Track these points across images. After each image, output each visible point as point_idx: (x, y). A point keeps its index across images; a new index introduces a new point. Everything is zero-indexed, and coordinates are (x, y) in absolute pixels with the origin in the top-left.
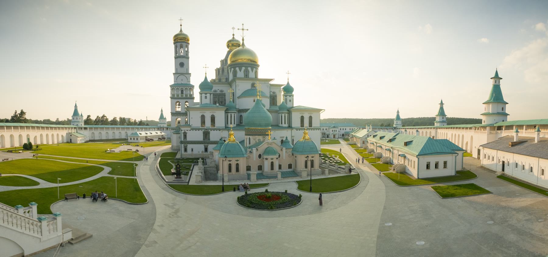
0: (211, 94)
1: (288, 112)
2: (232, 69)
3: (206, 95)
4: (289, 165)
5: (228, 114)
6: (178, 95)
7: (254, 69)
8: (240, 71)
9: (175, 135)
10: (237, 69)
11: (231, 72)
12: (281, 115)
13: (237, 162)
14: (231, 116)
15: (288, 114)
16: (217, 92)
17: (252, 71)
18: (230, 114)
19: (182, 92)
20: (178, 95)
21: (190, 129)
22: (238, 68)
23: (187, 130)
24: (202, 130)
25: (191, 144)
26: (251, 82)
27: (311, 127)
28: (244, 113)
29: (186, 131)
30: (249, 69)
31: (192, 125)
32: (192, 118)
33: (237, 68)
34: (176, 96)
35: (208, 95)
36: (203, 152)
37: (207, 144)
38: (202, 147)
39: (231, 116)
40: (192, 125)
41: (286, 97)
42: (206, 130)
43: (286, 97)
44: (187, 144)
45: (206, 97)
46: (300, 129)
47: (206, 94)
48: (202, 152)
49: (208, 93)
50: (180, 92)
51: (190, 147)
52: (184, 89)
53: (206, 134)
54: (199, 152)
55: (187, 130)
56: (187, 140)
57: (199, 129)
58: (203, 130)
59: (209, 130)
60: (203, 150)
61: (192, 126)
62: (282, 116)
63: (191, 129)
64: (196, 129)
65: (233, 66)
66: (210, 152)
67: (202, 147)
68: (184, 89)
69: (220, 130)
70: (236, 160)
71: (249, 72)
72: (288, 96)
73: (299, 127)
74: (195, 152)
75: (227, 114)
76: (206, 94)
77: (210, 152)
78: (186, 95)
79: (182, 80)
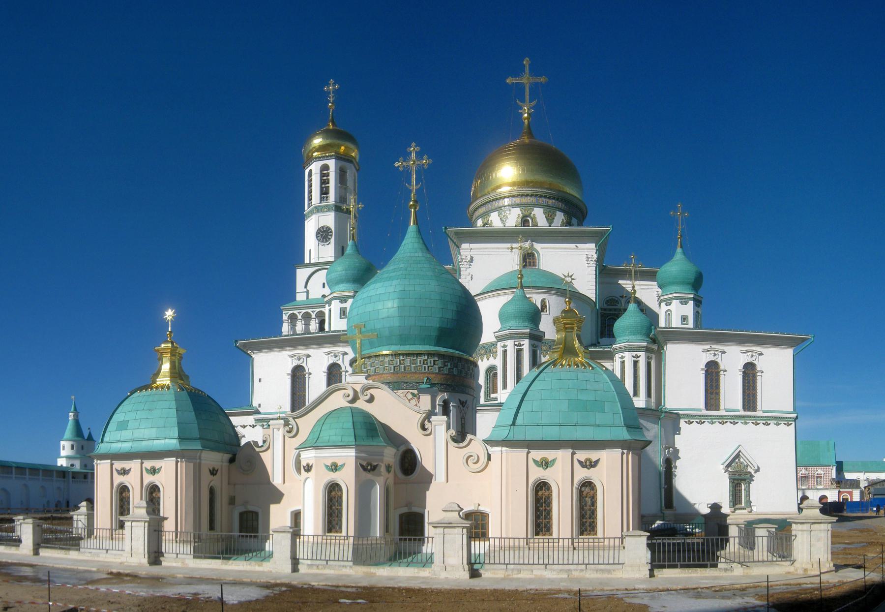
21: (253, 423)
23: (244, 427)
27: (754, 409)
31: (259, 405)
32: (260, 380)
40: (259, 405)
46: (701, 420)
55: (244, 427)
63: (257, 421)
73: (700, 410)
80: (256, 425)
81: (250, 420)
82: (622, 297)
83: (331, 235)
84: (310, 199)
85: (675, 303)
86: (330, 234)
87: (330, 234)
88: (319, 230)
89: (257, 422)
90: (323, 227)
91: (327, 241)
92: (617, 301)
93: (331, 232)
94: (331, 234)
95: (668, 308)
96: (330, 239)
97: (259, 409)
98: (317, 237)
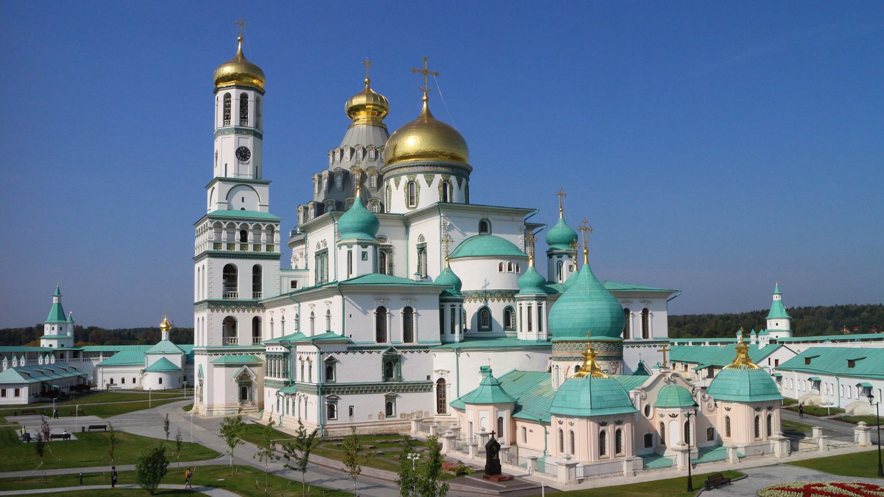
2: (404, 179)
3: (365, 250)
4: (645, 436)
5: (443, 304)
6: (230, 245)
7: (464, 181)
8: (427, 185)
9: (223, 369)
10: (421, 178)
11: (397, 184)
13: (617, 427)
14: (453, 310)
17: (460, 185)
18: (451, 304)
19: (243, 236)
20: (230, 245)
21: (345, 349)
22: (423, 175)
24: (379, 352)
25: (347, 393)
26: (479, 217)
28: (473, 302)
29: (335, 355)
30: (453, 179)
31: (351, 336)
33: (418, 175)
34: (224, 248)
35: (370, 250)
36: (383, 415)
37: (394, 390)
38: (379, 400)
39: (453, 310)
40: (351, 336)
42: (391, 350)
43: (561, 257)
44: (338, 392)
45: (364, 255)
48: (379, 416)
49: (371, 244)
50: (238, 235)
51: (344, 402)
52: (251, 227)
53: (391, 363)
54: (370, 416)
56: (337, 382)
57: (370, 349)
58: (383, 351)
59: (400, 351)
60: (383, 410)
61: (353, 339)
64: (361, 349)
65: (406, 170)
66: (401, 415)
67: (379, 400)
68: (251, 227)
69: (426, 348)
71: (451, 188)
74: (358, 418)
76: (364, 245)
77: (401, 415)
78: (257, 247)
79: (243, 201)
80: (348, 352)
81: (344, 348)
83: (250, 156)
84: (227, 117)
87: (248, 154)
89: (349, 349)
90: (242, 147)
91: (245, 160)
93: (250, 153)
95: (560, 259)
96: (248, 159)
97: (351, 339)
98: (237, 155)
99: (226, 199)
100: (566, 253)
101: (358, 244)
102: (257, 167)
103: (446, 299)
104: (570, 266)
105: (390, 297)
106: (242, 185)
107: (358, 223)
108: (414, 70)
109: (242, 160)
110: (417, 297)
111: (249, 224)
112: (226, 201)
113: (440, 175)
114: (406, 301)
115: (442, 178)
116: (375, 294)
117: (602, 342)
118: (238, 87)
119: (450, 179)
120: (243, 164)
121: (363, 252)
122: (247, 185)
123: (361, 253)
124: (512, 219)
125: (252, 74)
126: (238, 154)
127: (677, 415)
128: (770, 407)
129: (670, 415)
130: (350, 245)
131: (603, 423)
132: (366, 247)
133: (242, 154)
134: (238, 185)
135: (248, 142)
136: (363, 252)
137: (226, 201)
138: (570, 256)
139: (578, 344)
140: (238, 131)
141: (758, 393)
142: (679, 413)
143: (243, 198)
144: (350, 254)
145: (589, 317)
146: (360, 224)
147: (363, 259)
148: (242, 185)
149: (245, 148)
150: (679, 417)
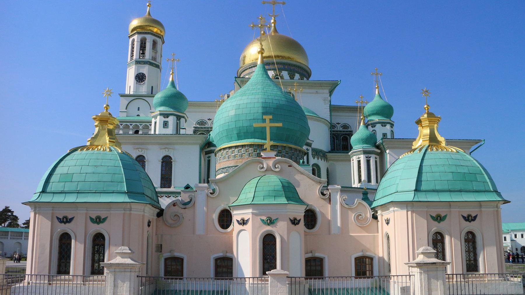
0: (179, 118)
1: (379, 151)
3: (166, 119)
12: (359, 158)
15: (378, 157)
16: (206, 126)
30: (285, 74)
35: (171, 120)
41: (372, 127)
45: (165, 125)
47: (166, 115)
62: (359, 162)
68: (141, 127)
70: (92, 219)
72: (380, 125)
75: (208, 156)
76: (166, 115)
82: (338, 124)
83: (145, 79)
84: (132, 56)
85: (378, 126)
86: (144, 78)
87: (144, 78)
88: (137, 75)
90: (140, 73)
92: (335, 126)
93: (145, 77)
94: (145, 78)
95: (374, 129)
96: (144, 81)
98: (136, 79)
99: (126, 109)
100: (379, 123)
101: (161, 114)
102: (152, 87)
103: (211, 150)
104: (383, 134)
105: (149, 147)
106: (138, 99)
107: (161, 98)
108: (264, 2)
109: (139, 82)
110: (177, 147)
111: (139, 125)
112: (126, 111)
113: (273, 71)
114: (164, 150)
115: (274, 74)
116: (134, 144)
117: (251, 146)
118: (139, 33)
119: (282, 74)
120: (140, 84)
121: (164, 121)
122: (142, 99)
123: (163, 122)
124: (317, 92)
125: (151, 24)
126: (136, 78)
127: (247, 221)
128: (469, 216)
129: (238, 221)
130: (155, 117)
131: (66, 217)
132: (167, 118)
133: (140, 78)
134: (133, 100)
135: (145, 70)
136: (164, 121)
137: (126, 111)
138: (384, 124)
139: (225, 152)
140: (137, 62)
141: (438, 188)
142: (250, 216)
143: (139, 108)
144: (156, 123)
145: (233, 114)
146: (163, 99)
147: (164, 127)
148: (138, 99)
149: (143, 74)
150: (250, 223)
